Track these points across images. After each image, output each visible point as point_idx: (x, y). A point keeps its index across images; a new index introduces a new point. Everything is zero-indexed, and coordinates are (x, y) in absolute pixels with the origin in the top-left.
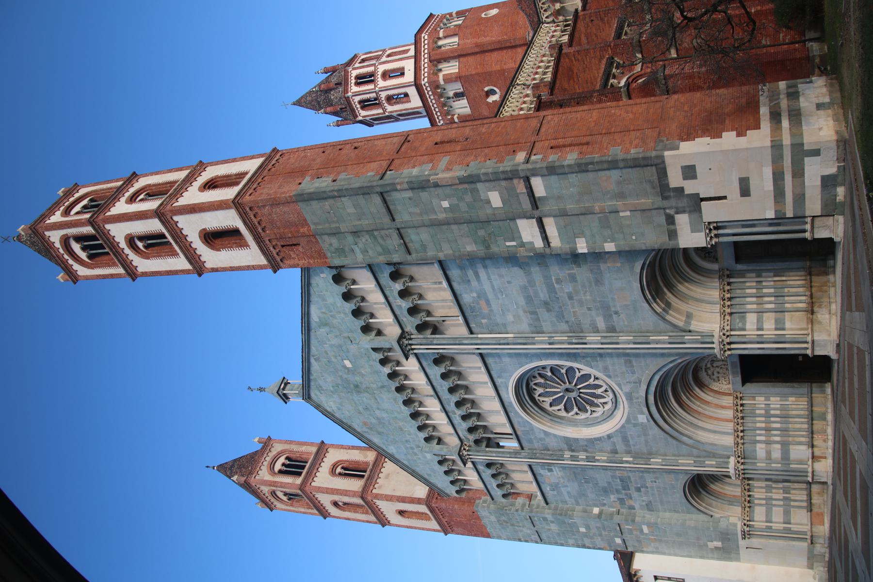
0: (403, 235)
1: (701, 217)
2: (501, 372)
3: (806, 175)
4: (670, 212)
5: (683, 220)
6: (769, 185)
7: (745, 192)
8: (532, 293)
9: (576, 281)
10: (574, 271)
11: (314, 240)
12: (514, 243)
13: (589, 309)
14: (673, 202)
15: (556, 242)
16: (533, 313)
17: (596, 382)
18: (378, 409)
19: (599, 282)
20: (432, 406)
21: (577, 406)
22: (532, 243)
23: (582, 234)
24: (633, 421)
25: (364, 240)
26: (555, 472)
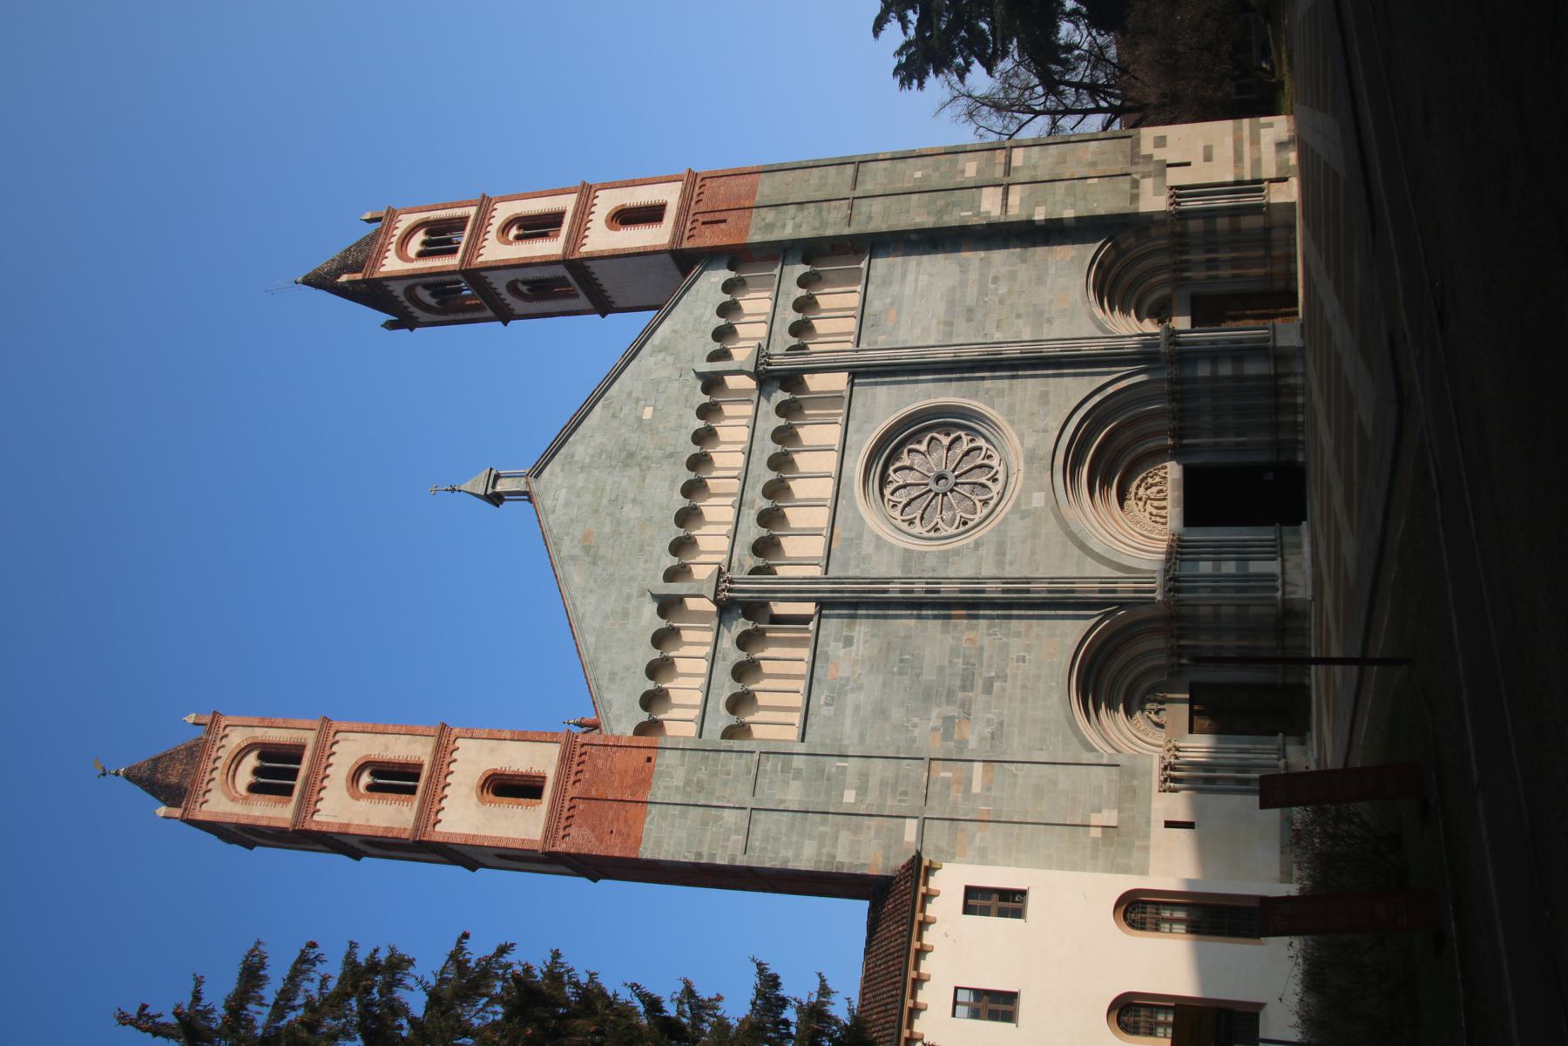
0: (854, 208)
2: (865, 422)
3: (1262, 142)
4: (1135, 176)
5: (1147, 184)
6: (1230, 154)
7: (1208, 158)
10: (1016, 268)
11: (746, 214)
12: (970, 213)
13: (1019, 316)
14: (1140, 168)
16: (949, 324)
17: (986, 461)
18: (634, 501)
19: (1040, 280)
20: (717, 511)
21: (941, 513)
22: (989, 212)
23: (1044, 203)
24: (1023, 507)
25: (805, 213)
26: (854, 648)
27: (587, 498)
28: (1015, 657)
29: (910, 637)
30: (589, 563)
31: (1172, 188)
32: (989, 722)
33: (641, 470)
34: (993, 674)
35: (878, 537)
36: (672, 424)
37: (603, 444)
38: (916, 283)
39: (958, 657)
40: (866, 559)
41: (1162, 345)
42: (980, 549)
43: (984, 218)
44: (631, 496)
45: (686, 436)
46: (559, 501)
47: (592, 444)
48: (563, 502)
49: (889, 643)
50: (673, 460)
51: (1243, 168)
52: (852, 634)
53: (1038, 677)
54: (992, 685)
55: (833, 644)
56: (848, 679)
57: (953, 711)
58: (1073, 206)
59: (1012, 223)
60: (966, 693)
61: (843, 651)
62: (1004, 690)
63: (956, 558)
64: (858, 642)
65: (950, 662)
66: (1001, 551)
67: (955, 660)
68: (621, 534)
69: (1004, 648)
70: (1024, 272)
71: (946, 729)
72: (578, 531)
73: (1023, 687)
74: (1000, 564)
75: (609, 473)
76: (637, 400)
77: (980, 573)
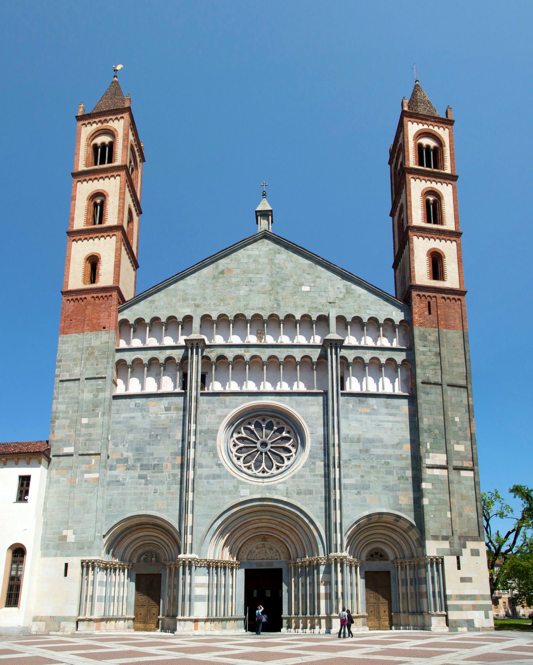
1: (447, 555)
5: (445, 545)
8: (376, 444)
9: (387, 474)
15: (429, 472)
19: (386, 487)
23: (434, 488)
24: (240, 486)
26: (165, 412)
27: (253, 266)
28: (157, 488)
29: (169, 438)
30: (214, 275)
31: (443, 559)
32: (125, 479)
33: (270, 291)
34: (148, 478)
35: (225, 416)
36: (299, 302)
37: (287, 268)
38: (387, 422)
39: (158, 461)
40: (213, 411)
41: (335, 554)
42: (217, 467)
43: (425, 455)
44: (254, 288)
45: (290, 311)
46: (251, 251)
47: (286, 262)
48: (250, 253)
49: (166, 428)
50: (275, 306)
51: (456, 600)
52: (172, 411)
53: (146, 500)
54: (143, 479)
55: (167, 402)
56: (148, 412)
57: (131, 462)
58: (431, 503)
59: (420, 470)
60: (139, 467)
61: (163, 407)
62: (140, 484)
63: (212, 455)
64: (167, 414)
65: (156, 458)
66: (215, 477)
67: (156, 460)
68: (231, 288)
69: (162, 482)
70: (392, 480)
71: (122, 460)
72: (232, 265)
73: (142, 493)
74: (208, 477)
75: (268, 275)
76: (314, 282)
77: (199, 468)
